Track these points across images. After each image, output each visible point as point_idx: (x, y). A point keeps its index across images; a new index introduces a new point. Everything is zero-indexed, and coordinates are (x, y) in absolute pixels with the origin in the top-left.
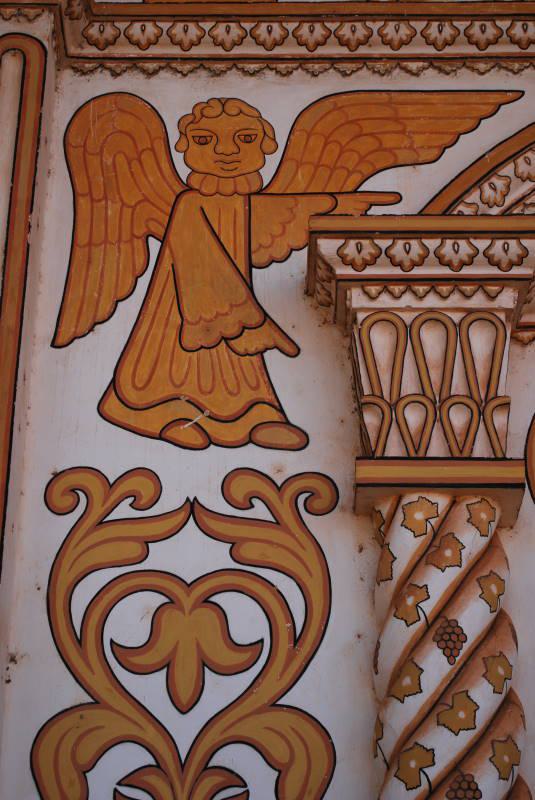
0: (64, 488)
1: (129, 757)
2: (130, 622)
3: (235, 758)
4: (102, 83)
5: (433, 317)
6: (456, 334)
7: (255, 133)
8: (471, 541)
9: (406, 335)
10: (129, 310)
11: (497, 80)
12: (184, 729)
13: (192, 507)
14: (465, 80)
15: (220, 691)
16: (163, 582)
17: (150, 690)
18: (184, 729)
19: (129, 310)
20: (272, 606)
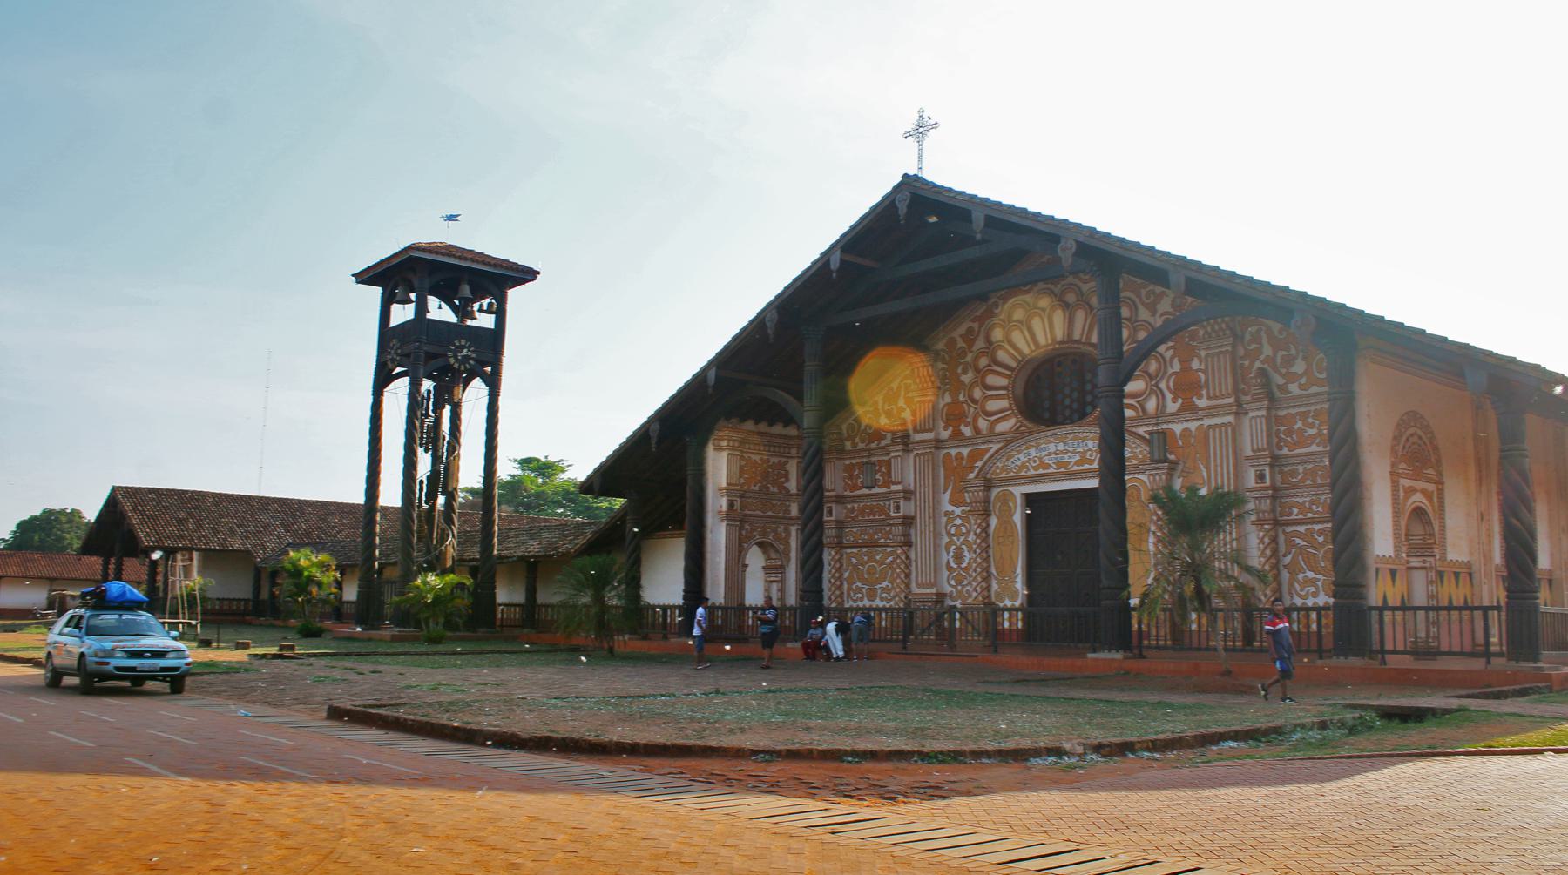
0: (947, 513)
1: (954, 547)
2: (953, 531)
3: (964, 546)
4: (946, 451)
5: (975, 491)
6: (978, 492)
7: (962, 458)
8: (979, 521)
9: (973, 493)
10: (950, 488)
11: (991, 445)
12: (958, 543)
13: (958, 516)
14: (985, 446)
15: (962, 538)
16: (955, 525)
17: (955, 538)
18: (958, 543)
19: (950, 488)
20: (966, 528)
